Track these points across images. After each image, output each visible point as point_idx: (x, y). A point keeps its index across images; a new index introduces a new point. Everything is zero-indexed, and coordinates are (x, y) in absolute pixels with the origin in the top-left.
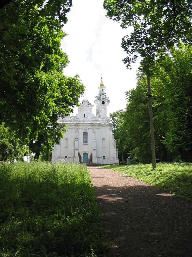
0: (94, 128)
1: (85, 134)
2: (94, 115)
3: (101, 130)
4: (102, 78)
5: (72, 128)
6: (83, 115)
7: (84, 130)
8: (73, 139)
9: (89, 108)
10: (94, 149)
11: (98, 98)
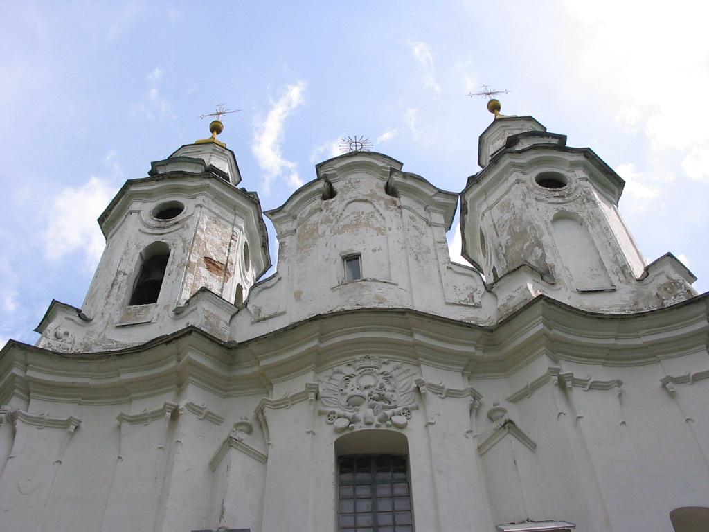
0: (494, 392)
3: (611, 397)
6: (338, 270)
7: (354, 402)
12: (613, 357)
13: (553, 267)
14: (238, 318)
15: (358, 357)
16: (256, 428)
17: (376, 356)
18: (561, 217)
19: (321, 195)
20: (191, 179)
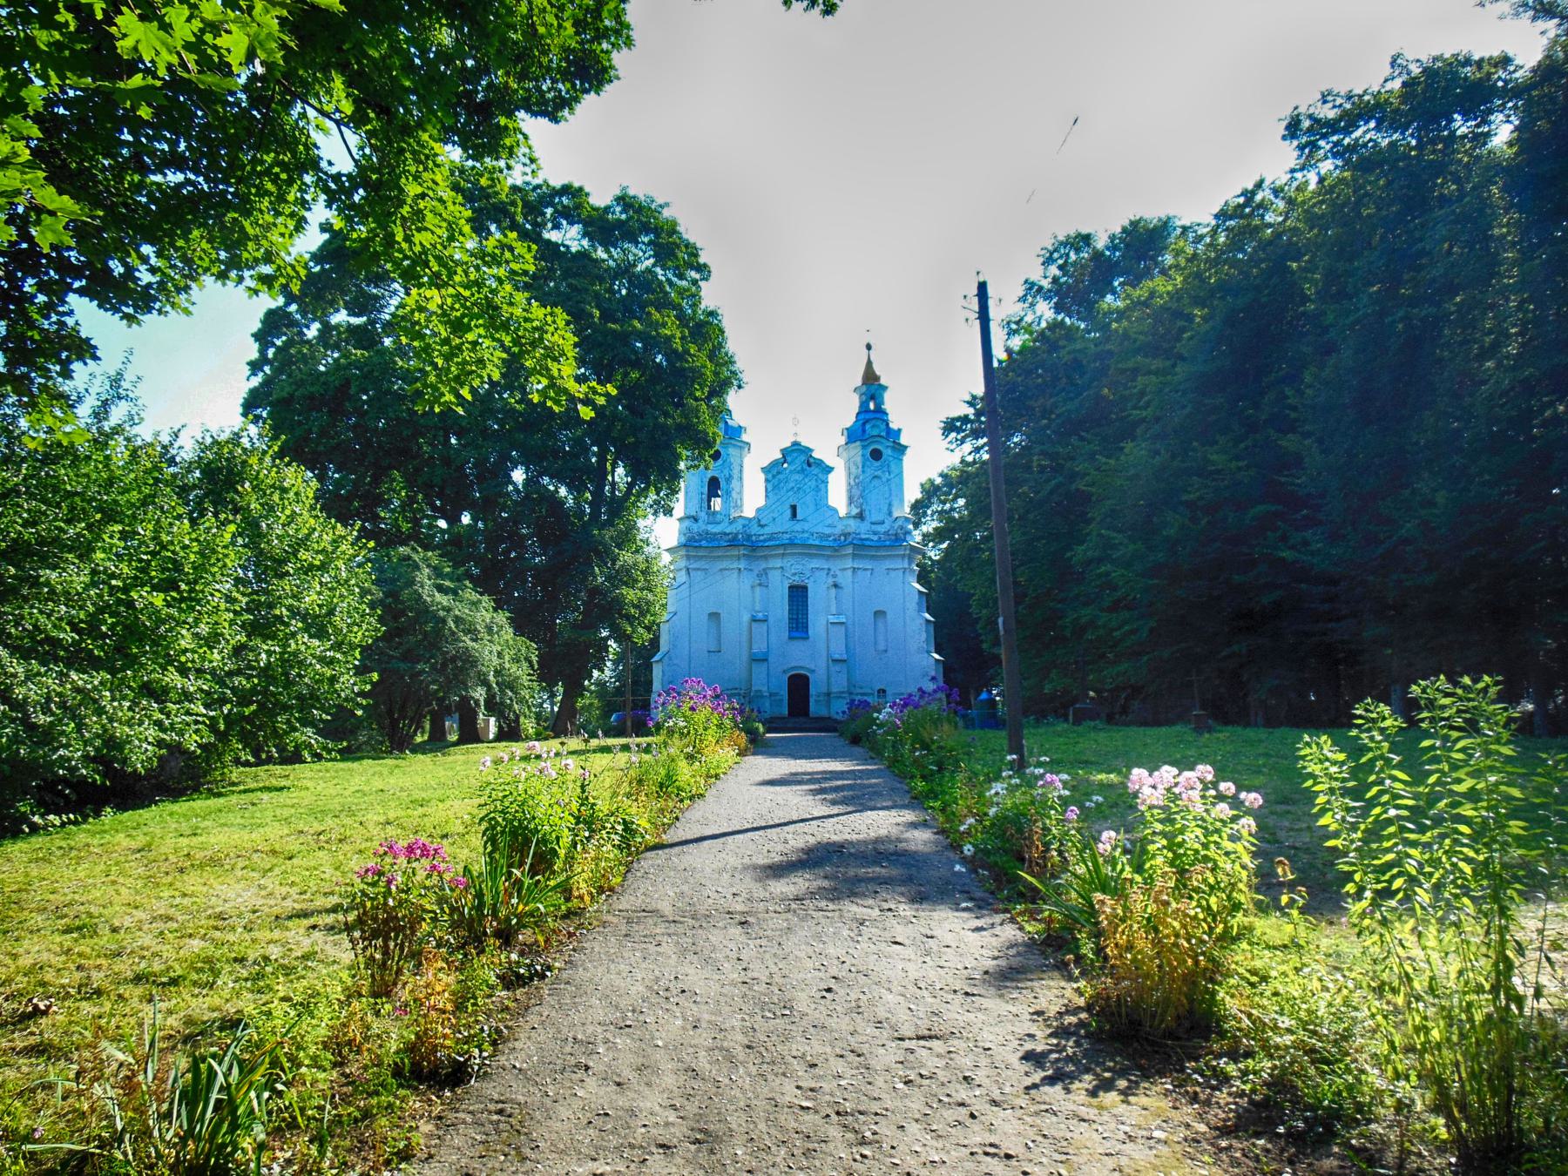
0: (836, 566)
1: (798, 594)
2: (835, 511)
4: (869, 347)
6: (789, 512)
8: (746, 618)
10: (837, 656)
11: (854, 435)
12: (873, 557)
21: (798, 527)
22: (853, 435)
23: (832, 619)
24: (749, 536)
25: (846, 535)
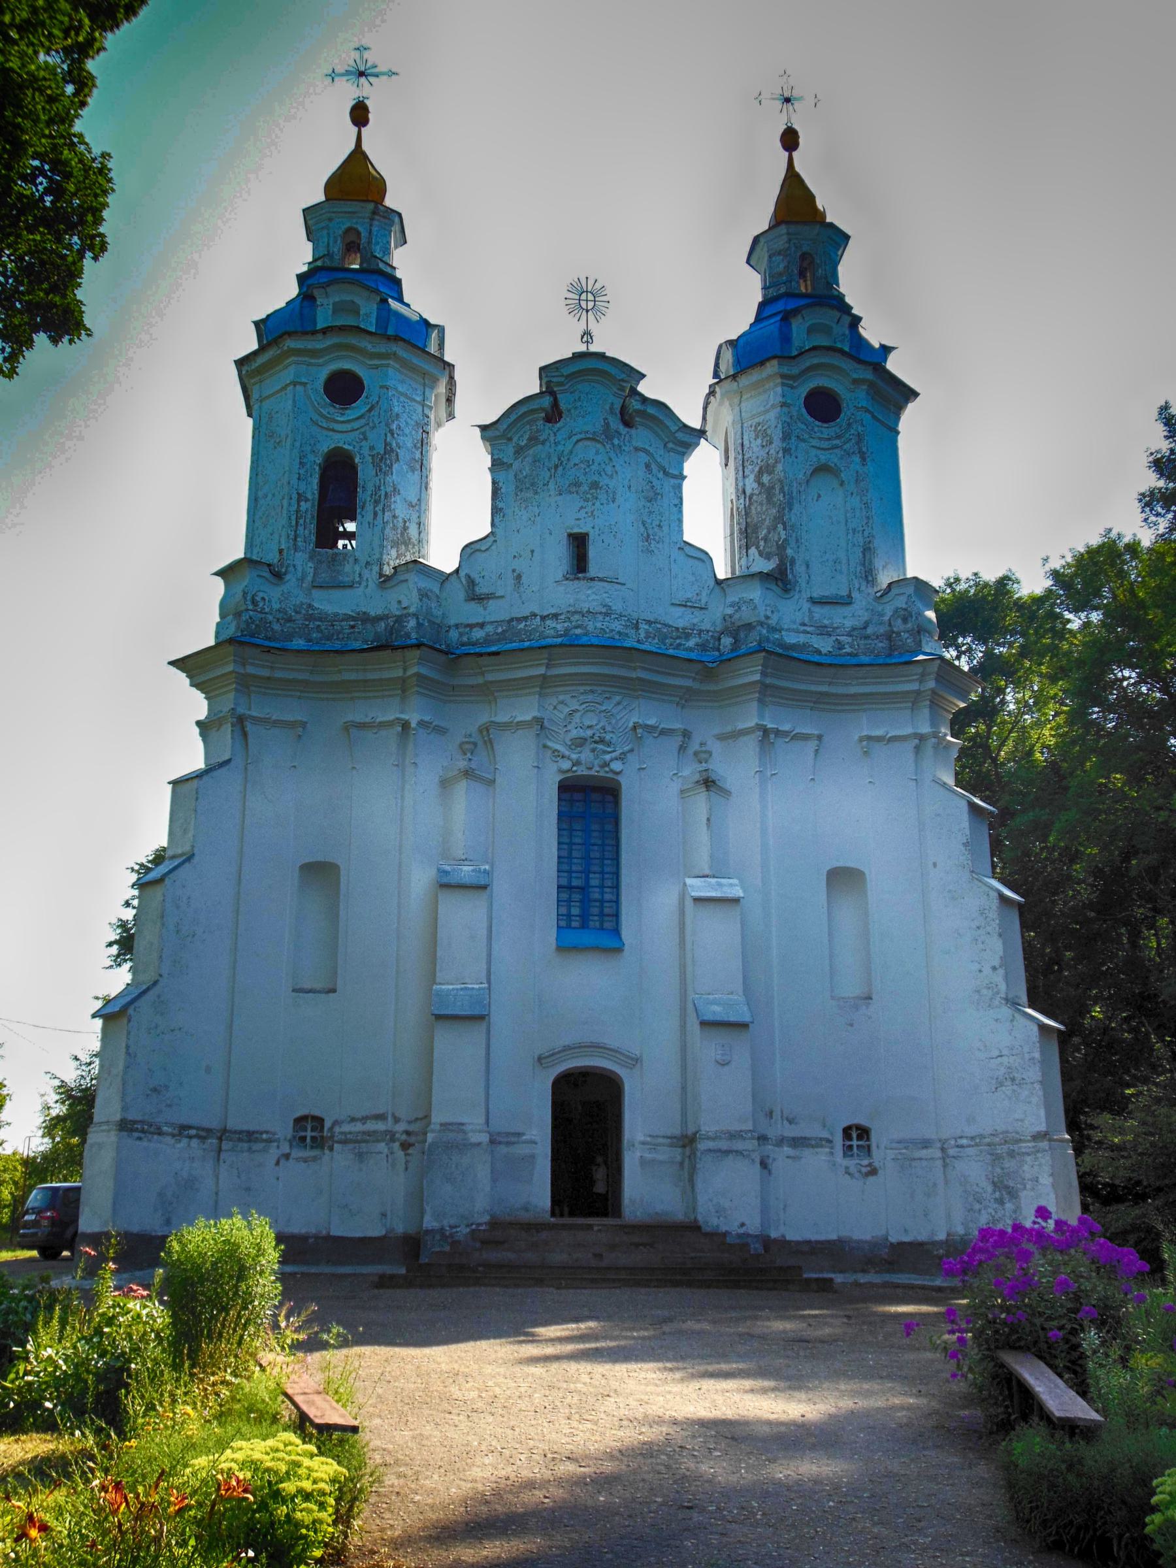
2: (703, 558)
4: (790, 140)
5: (405, 725)
9: (643, 458)
10: (716, 1011)
12: (820, 702)
13: (793, 562)
14: (447, 585)
15: (582, 689)
16: (480, 743)
17: (600, 689)
18: (822, 469)
19: (543, 415)
20: (368, 337)
21: (587, 596)
22: (744, 358)
23: (698, 887)
24: (439, 628)
25: (737, 631)
